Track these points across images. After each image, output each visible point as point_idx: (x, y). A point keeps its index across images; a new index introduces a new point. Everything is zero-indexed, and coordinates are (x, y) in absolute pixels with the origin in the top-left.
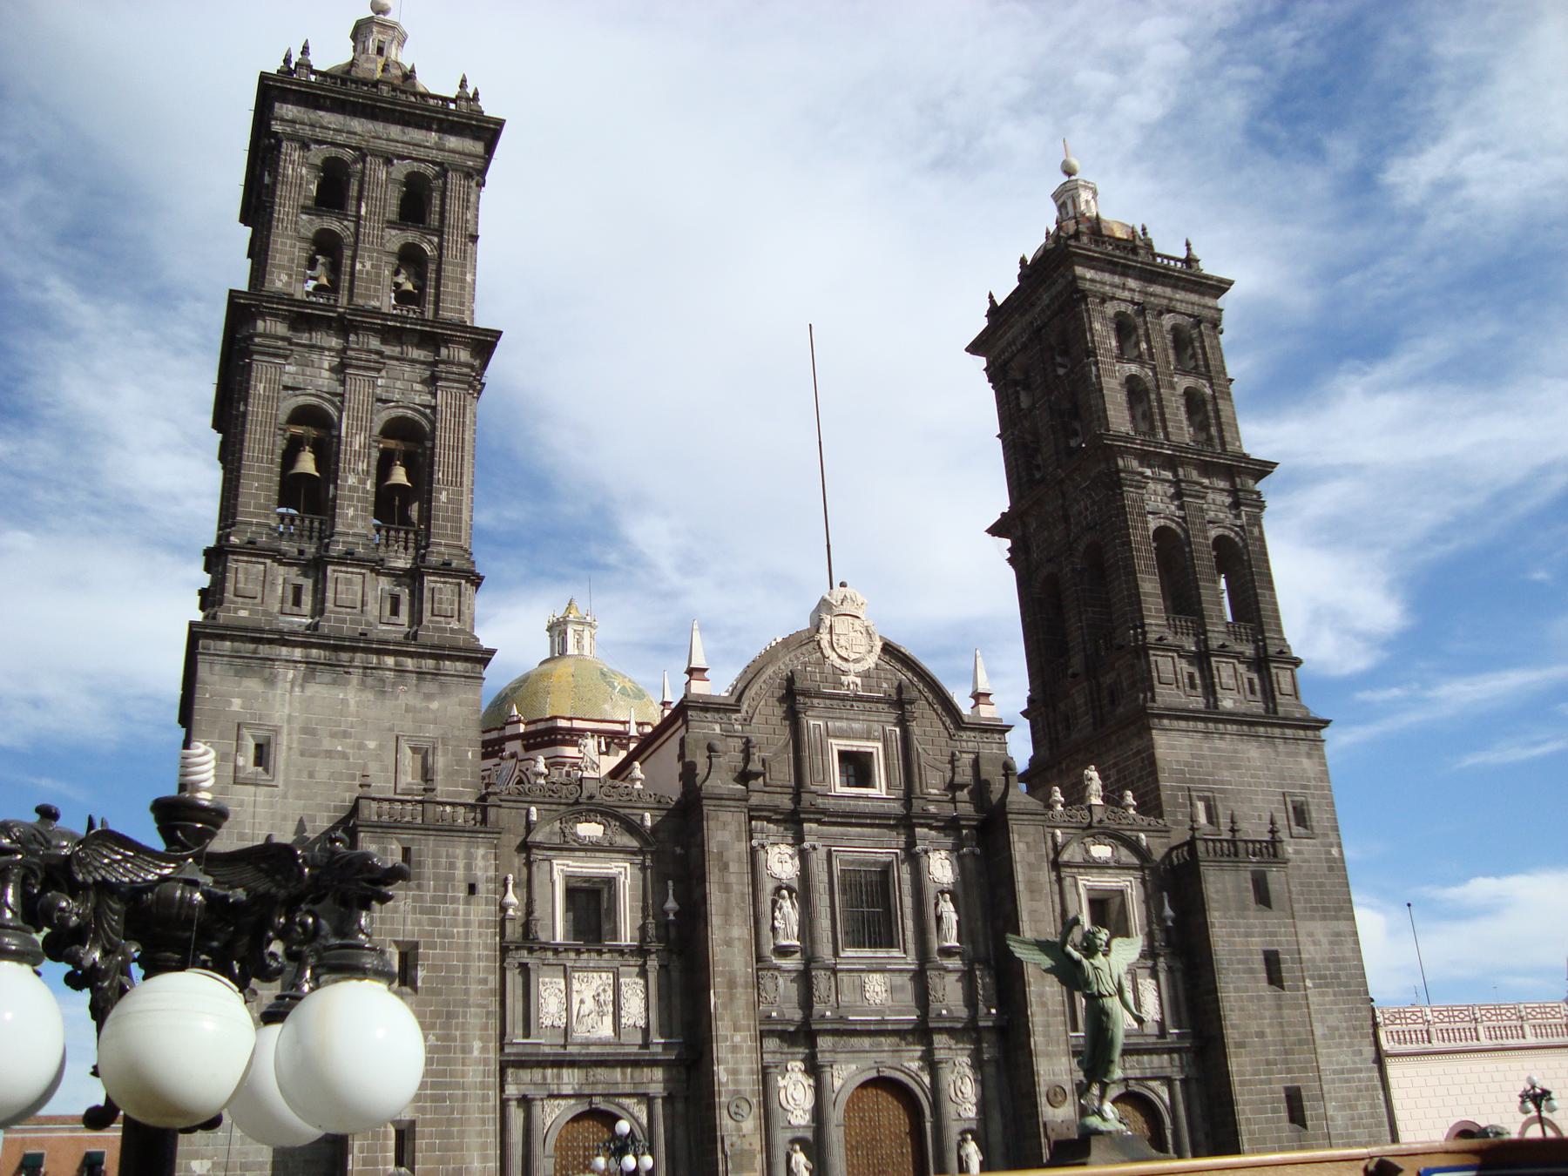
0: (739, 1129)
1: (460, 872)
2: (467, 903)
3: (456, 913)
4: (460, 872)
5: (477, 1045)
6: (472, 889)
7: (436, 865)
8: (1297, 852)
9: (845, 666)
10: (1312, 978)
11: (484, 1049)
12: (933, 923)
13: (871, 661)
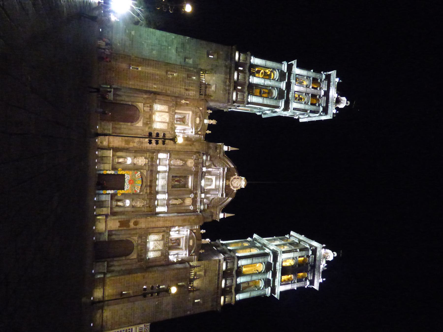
0: (134, 142)
1: (191, 88)
2: (184, 89)
3: (182, 86)
4: (191, 88)
5: (156, 86)
6: (187, 90)
7: (192, 83)
8: (189, 300)
9: (231, 181)
10: (158, 304)
11: (155, 88)
12: (176, 197)
13: (232, 187)
